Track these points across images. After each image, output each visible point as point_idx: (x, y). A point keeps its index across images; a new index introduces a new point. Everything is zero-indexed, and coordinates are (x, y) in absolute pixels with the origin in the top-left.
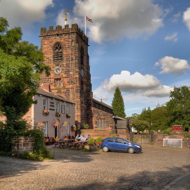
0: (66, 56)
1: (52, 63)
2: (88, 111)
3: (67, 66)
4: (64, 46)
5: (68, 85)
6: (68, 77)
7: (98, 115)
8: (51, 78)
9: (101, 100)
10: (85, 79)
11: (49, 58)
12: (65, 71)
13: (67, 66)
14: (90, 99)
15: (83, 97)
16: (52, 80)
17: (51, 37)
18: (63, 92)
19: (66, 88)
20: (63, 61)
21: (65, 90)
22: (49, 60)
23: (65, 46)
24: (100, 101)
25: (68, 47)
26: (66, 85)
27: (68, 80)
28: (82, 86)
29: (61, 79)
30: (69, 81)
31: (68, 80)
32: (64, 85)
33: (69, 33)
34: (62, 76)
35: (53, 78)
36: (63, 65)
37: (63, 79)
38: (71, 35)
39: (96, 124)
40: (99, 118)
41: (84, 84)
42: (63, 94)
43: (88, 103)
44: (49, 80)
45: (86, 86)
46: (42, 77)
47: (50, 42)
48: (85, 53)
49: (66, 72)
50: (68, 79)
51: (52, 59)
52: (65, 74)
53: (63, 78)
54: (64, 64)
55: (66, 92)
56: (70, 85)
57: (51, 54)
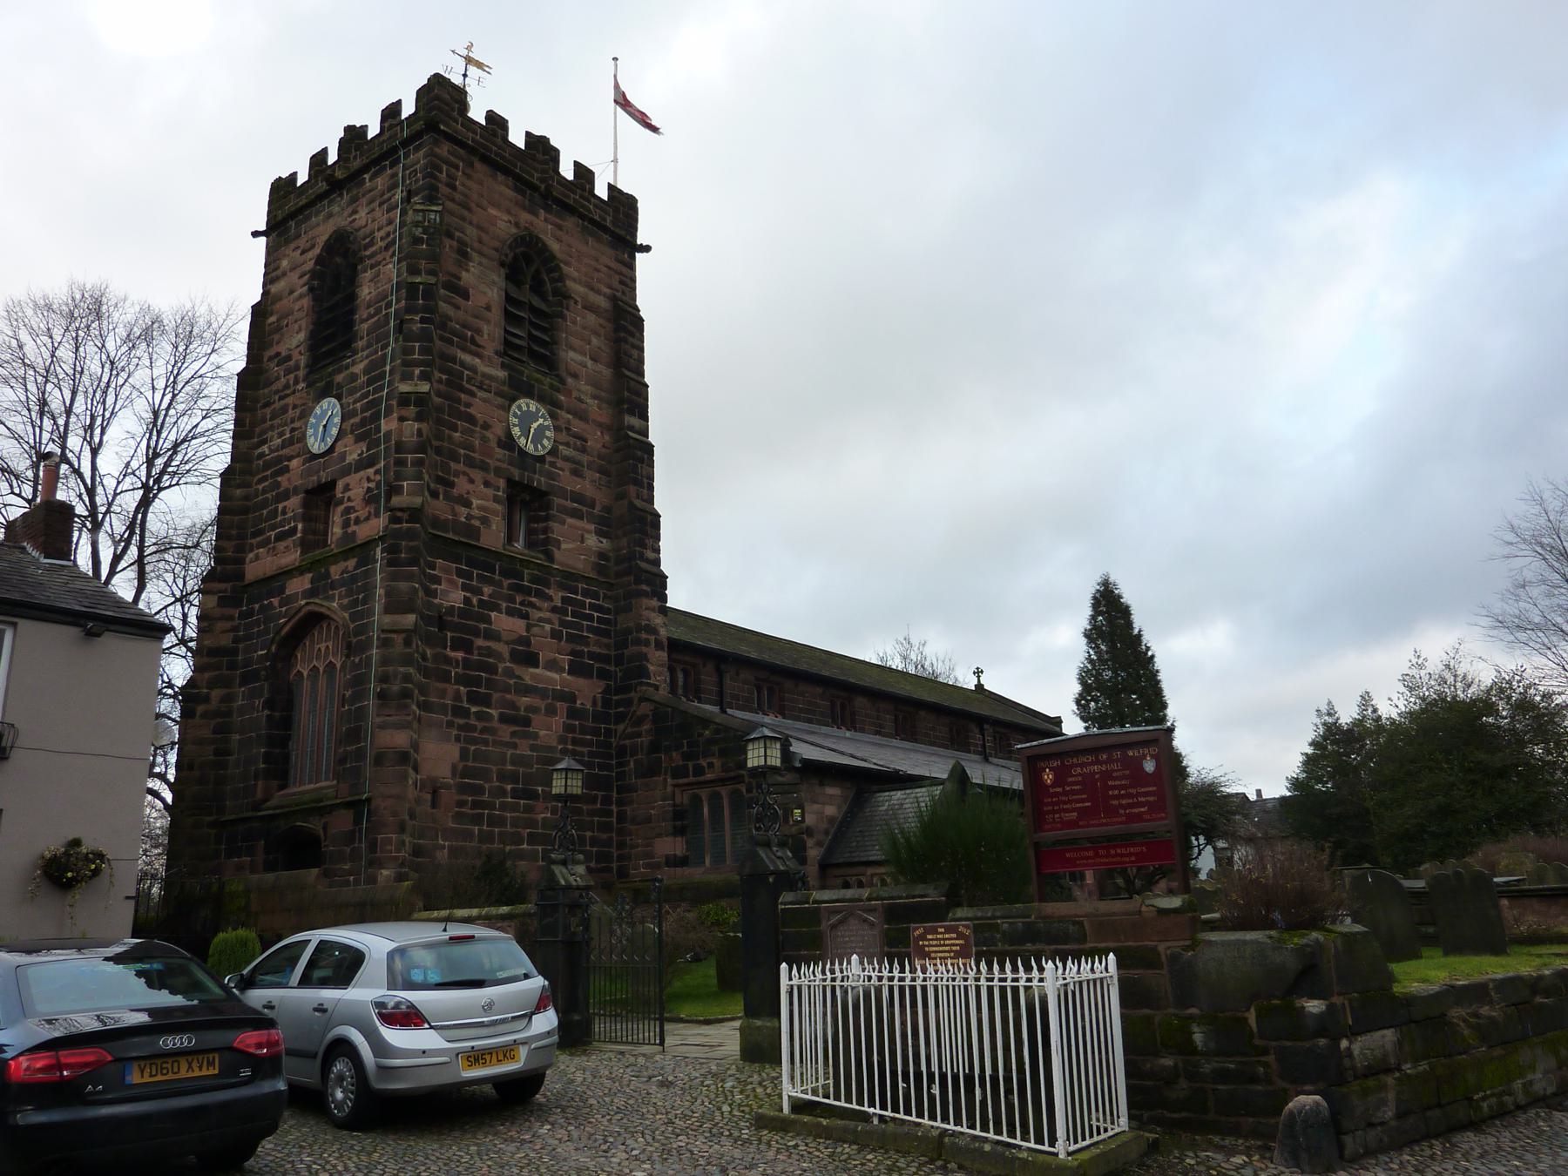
0: (372, 310)
1: (301, 385)
2: (621, 727)
3: (369, 383)
4: (366, 247)
5: (367, 519)
6: (369, 462)
7: (687, 757)
8: (285, 496)
9: (978, 672)
10: (576, 473)
11: (289, 358)
12: (357, 420)
13: (369, 383)
14: (631, 624)
15: (535, 614)
16: (294, 503)
17: (308, 218)
18: (342, 582)
19: (359, 542)
20: (355, 352)
21: (352, 563)
22: (288, 372)
23: (371, 244)
24: (970, 683)
25: (387, 248)
26: (357, 521)
27: (369, 480)
28: (546, 530)
29: (331, 485)
30: (372, 485)
31: (369, 480)
32: (346, 524)
33: (394, 150)
34: (343, 456)
35: (296, 491)
36: (354, 377)
37: (347, 479)
38: (406, 156)
39: (679, 832)
40: (692, 779)
41: (577, 514)
42: (341, 597)
43: (619, 660)
44: (280, 506)
45: (600, 533)
46: (246, 498)
47: (303, 253)
48: (570, 284)
49: (363, 422)
50: (371, 471)
51: (303, 361)
52: (359, 439)
53: (346, 471)
54: (362, 366)
55: (354, 579)
56: (377, 515)
57: (300, 330)
